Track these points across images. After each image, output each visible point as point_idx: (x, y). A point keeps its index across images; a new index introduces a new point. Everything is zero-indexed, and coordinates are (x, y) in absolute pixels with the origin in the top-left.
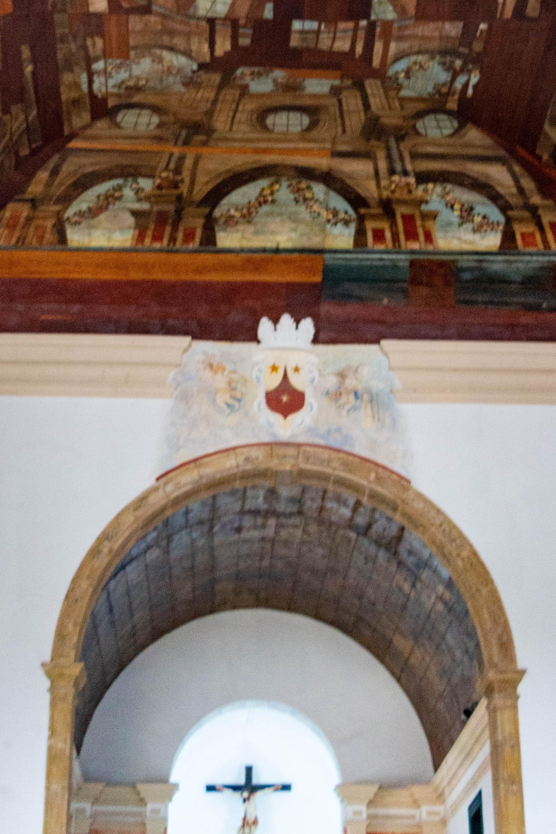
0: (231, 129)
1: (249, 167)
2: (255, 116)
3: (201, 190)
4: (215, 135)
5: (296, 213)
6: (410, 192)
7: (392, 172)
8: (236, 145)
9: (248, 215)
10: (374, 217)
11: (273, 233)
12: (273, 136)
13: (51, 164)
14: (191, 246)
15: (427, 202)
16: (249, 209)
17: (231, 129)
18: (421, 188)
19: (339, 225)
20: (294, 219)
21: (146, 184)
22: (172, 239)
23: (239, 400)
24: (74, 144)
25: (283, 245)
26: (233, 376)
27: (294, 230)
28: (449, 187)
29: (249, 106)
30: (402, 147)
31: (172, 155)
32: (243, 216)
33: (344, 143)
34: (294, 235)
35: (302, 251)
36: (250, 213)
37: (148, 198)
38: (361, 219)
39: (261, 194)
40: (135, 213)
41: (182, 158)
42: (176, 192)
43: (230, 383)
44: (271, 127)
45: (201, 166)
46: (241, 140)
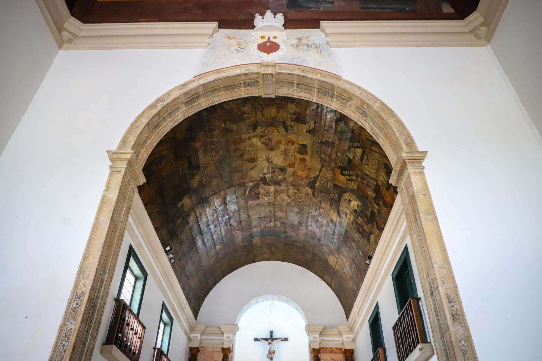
26: (240, 41)
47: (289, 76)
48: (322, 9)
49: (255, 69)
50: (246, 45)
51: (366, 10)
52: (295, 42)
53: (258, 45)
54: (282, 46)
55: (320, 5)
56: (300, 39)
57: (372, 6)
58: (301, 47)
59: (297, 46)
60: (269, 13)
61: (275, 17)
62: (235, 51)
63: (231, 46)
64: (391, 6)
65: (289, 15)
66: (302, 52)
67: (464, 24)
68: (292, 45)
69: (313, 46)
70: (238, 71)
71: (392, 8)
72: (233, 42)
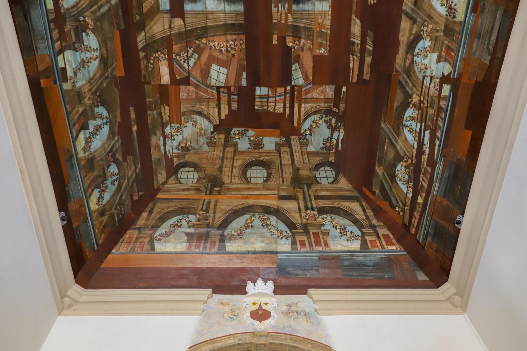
0: (231, 182)
1: (240, 207)
2: (242, 170)
3: (218, 221)
4: (224, 186)
5: (263, 233)
6: (316, 220)
7: (307, 209)
8: (234, 193)
9: (240, 235)
10: (300, 234)
11: (252, 243)
12: (250, 186)
13: (148, 209)
14: (213, 251)
15: (324, 225)
16: (240, 231)
17: (231, 182)
18: (321, 217)
19: (284, 239)
20: (261, 235)
21: (193, 218)
22: (205, 248)
23: (236, 316)
24: (160, 196)
25: (257, 250)
27: (262, 242)
28: (334, 216)
29: (238, 163)
30: (310, 192)
31: (204, 200)
32: (238, 235)
33: (284, 190)
34: (263, 245)
35: (266, 252)
36: (241, 233)
37: (193, 226)
38: (294, 235)
39: (246, 223)
40: (187, 234)
41: (209, 203)
42: (206, 222)
43: (231, 310)
44: (249, 179)
45: (218, 207)
46: (236, 189)
47: (281, 346)
48: (308, 276)
49: (247, 339)
50: (239, 312)
51: (349, 277)
52: (285, 308)
53: (251, 312)
54: (273, 314)
55: (306, 273)
56: (289, 306)
57: (354, 274)
58: (291, 314)
59: (287, 313)
60: (260, 282)
61: (265, 285)
62: (229, 318)
63: (225, 312)
64: (371, 274)
65: (278, 281)
66: (292, 320)
67: (439, 292)
68: (282, 312)
69: (302, 313)
70: (231, 341)
71: (372, 276)
72: (227, 309)
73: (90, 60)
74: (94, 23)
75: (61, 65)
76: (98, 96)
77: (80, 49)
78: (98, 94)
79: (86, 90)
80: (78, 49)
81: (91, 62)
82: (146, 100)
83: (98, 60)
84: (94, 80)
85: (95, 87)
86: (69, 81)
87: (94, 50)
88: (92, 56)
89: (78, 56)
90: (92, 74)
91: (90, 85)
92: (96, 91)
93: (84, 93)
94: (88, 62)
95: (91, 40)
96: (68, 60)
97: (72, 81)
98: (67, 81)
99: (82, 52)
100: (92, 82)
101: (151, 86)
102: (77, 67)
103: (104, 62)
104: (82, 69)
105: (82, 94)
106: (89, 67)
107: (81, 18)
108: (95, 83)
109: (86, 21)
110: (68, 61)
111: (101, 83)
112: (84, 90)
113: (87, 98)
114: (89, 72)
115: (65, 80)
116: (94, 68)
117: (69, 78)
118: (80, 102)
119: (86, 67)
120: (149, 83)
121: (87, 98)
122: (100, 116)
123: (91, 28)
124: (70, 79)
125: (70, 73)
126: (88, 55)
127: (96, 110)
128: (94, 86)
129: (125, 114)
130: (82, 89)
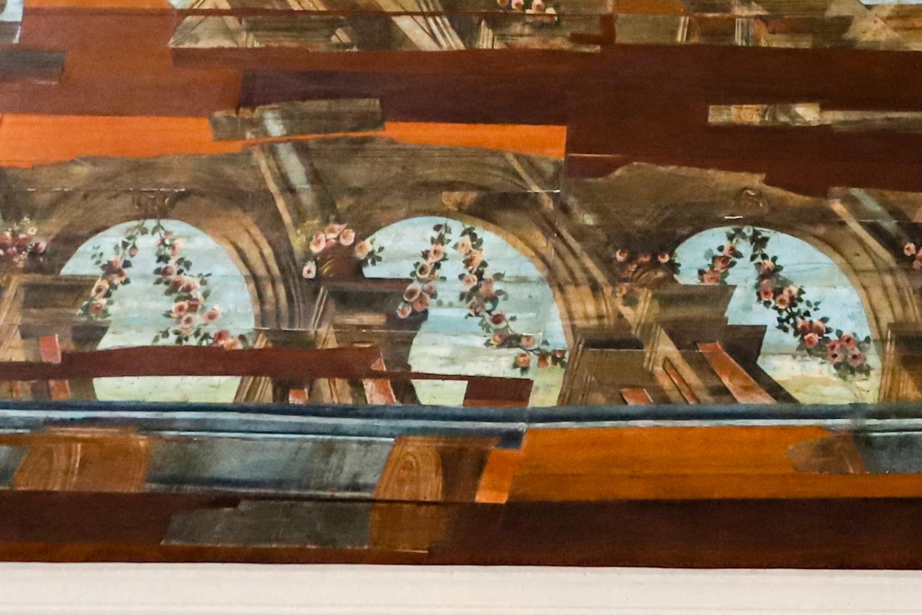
73: (477, 262)
74: (339, 221)
75: (452, 395)
76: (630, 260)
77: (421, 299)
78: (620, 257)
79: (591, 309)
80: (419, 308)
81: (484, 264)
82: (681, 48)
83: (480, 232)
84: (559, 263)
85: (590, 264)
86: (529, 376)
87: (441, 240)
88: (460, 255)
89: (445, 312)
90: (533, 270)
91: (577, 285)
92: (607, 263)
93: (600, 317)
94: (480, 275)
95: (398, 245)
96: (448, 356)
97: (534, 359)
98: (529, 382)
99: (433, 295)
100: (563, 273)
101: (622, 15)
102: (486, 327)
103: (495, 205)
104: (501, 308)
105: (601, 327)
106: (498, 277)
107: (309, 270)
108: (572, 262)
109: (325, 253)
110: (452, 360)
111: (581, 234)
112: (587, 317)
113: (627, 311)
114: (521, 280)
115: (519, 389)
116: (511, 252)
117: (516, 374)
118: (638, 345)
119: (496, 286)
120: (608, 21)
121: (627, 311)
122: (719, 266)
123: (352, 235)
124: (524, 369)
125: (499, 365)
126: (452, 269)
127: (687, 277)
128: (585, 270)
129: (738, 148)
130: (580, 323)
